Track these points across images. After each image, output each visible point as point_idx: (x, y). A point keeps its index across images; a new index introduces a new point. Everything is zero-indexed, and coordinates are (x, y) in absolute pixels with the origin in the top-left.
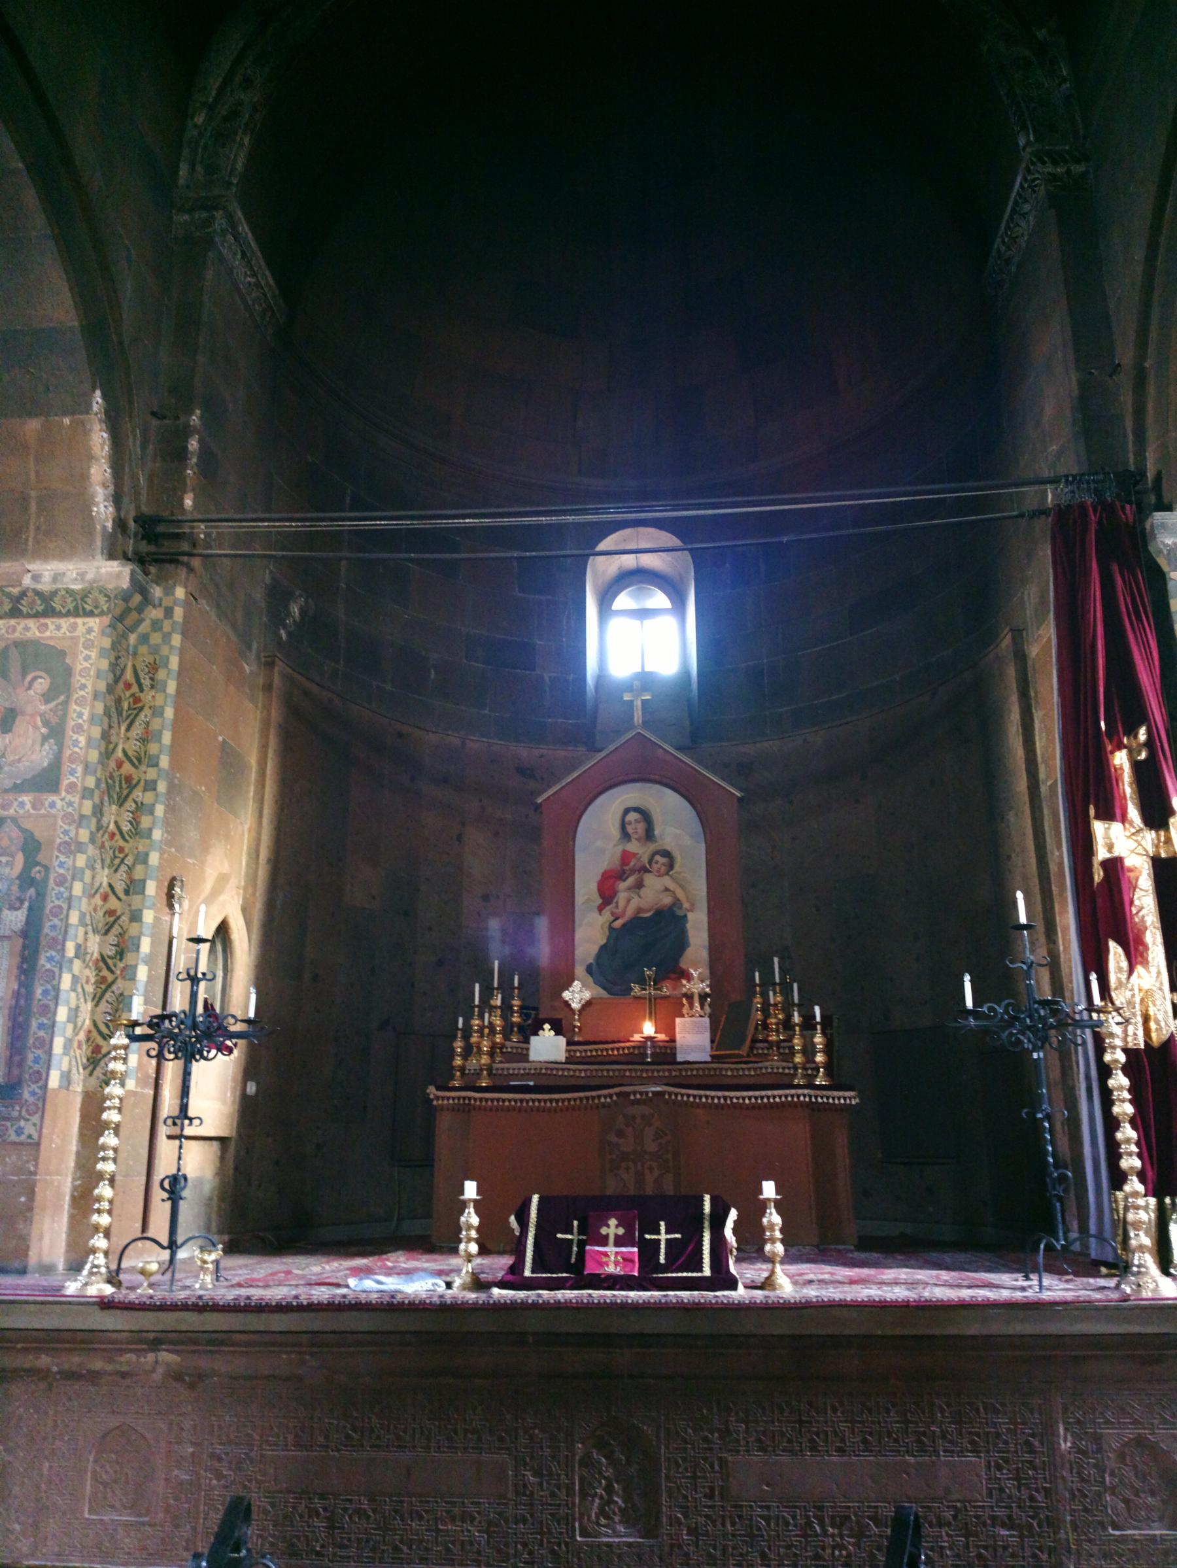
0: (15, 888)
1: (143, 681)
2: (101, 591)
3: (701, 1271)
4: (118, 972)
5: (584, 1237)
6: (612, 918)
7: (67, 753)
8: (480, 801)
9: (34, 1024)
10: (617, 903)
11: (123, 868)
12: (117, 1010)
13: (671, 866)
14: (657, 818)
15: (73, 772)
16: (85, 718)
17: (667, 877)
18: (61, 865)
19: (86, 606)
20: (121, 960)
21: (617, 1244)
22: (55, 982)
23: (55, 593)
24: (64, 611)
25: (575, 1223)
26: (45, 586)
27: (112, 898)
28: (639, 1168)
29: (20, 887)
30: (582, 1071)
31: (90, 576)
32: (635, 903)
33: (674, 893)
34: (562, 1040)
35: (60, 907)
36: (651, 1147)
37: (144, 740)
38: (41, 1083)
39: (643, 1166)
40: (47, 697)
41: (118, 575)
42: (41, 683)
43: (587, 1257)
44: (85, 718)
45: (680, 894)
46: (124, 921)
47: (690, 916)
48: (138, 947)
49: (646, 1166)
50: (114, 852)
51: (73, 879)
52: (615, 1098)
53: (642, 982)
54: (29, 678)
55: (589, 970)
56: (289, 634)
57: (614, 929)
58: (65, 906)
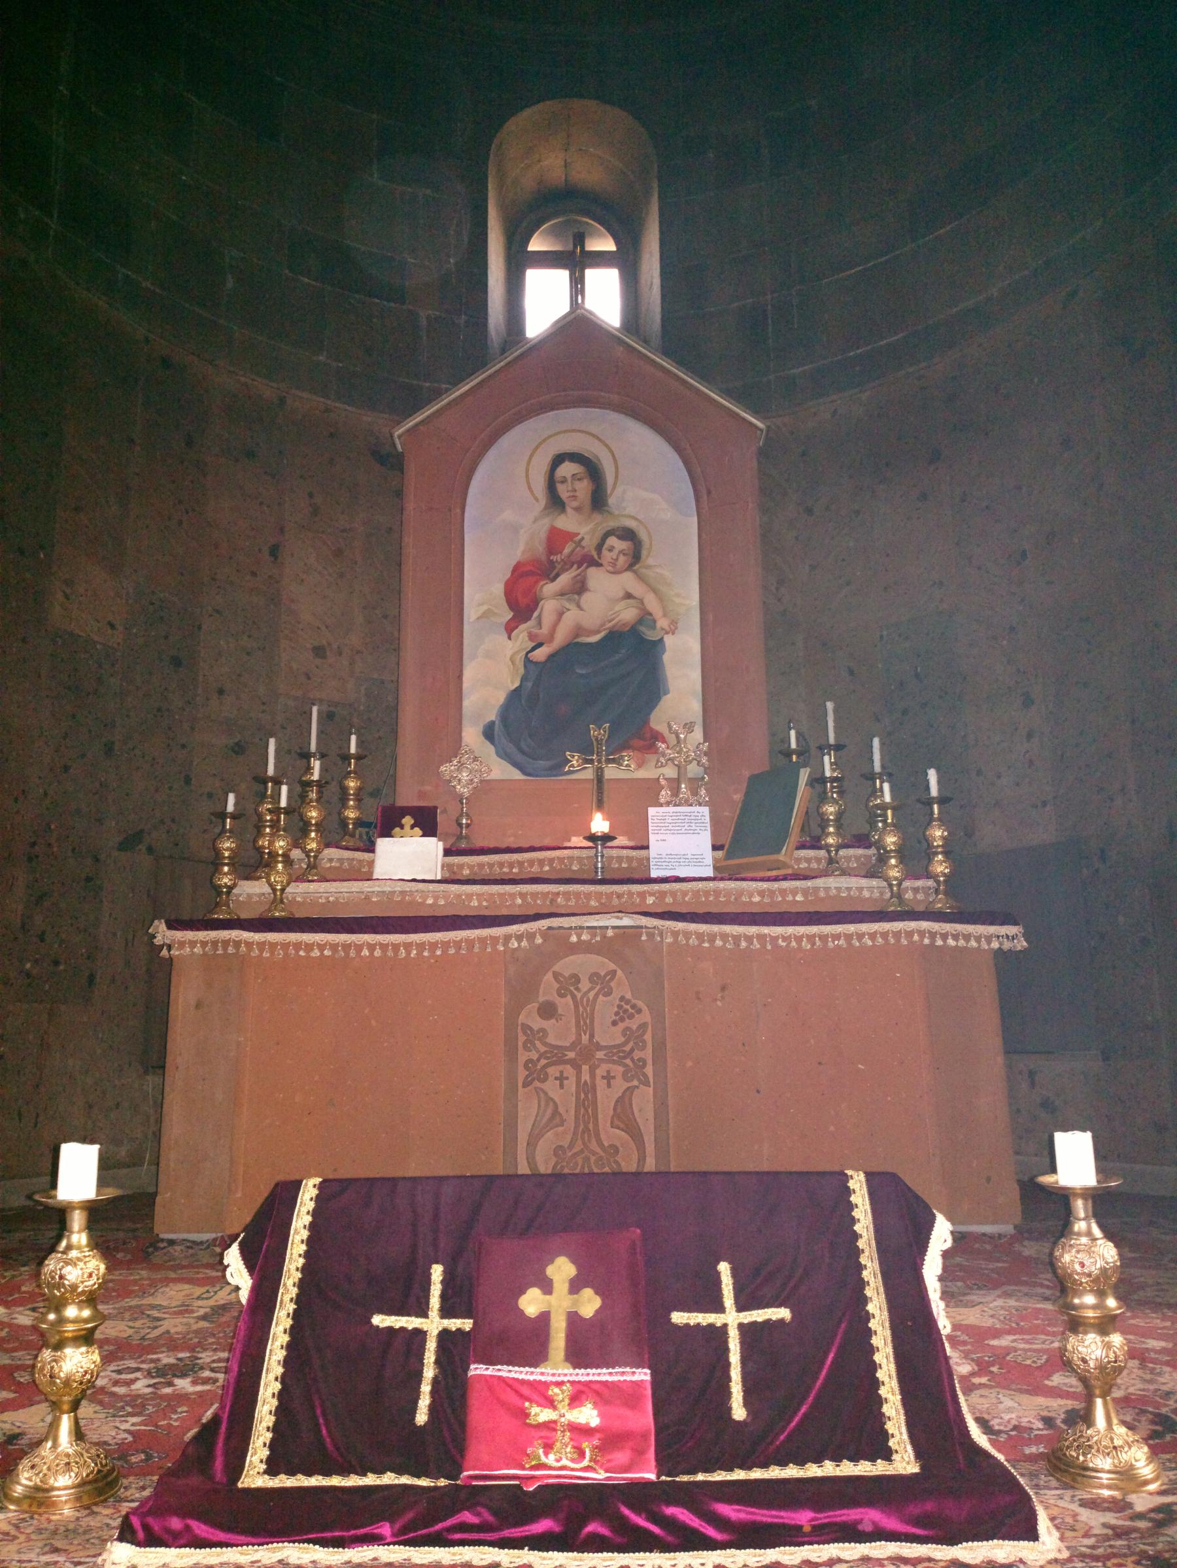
3: (887, 1454)
5: (467, 1324)
6: (531, 645)
8: (311, 495)
10: (539, 617)
13: (635, 557)
14: (610, 478)
17: (628, 576)
21: (578, 1355)
25: (437, 1272)
28: (586, 1077)
30: (475, 898)
32: (572, 617)
33: (642, 602)
34: (434, 846)
36: (608, 1035)
39: (593, 1075)
43: (479, 1416)
45: (652, 604)
47: (669, 640)
49: (600, 1072)
52: (539, 940)
53: (587, 750)
55: (489, 733)
57: (536, 663)
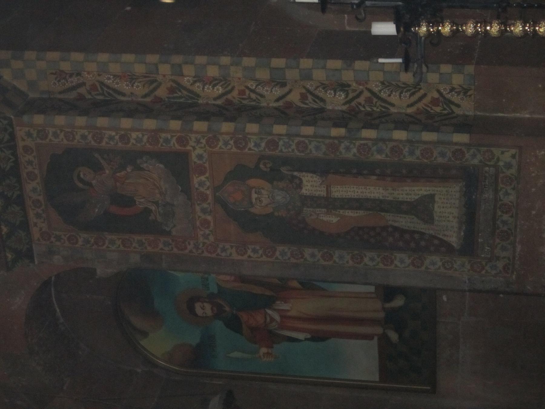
1: (74, 84)
4: (361, 87)
9: (409, 159)
11: (260, 90)
12: (398, 86)
15: (167, 141)
16: (113, 134)
18: (257, 145)
19: (5, 140)
20: (349, 86)
22: (370, 143)
24: (13, 159)
27: (289, 98)
35: (298, 144)
37: (132, 79)
38: (464, 149)
40: (97, 168)
42: (84, 174)
44: (113, 134)
46: (311, 85)
48: (336, 70)
50: (243, 99)
51: (271, 134)
54: (80, 185)
58: (297, 139)
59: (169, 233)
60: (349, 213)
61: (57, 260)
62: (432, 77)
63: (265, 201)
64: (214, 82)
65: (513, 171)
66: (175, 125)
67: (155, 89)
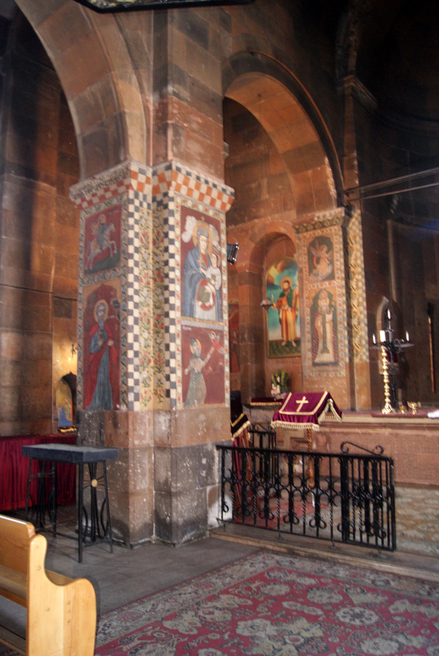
0: (328, 309)
2: (338, 218)
7: (335, 268)
9: (339, 345)
15: (338, 273)
23: (324, 221)
26: (321, 220)
29: (330, 308)
31: (333, 214)
37: (356, 260)
40: (327, 252)
41: (341, 212)
56: (394, 211)
59: (309, 275)
60: (321, 330)
61: (297, 241)
62: (364, 350)
63: (322, 304)
64: (357, 285)
65: (339, 375)
66: (343, 275)
67: (353, 267)
